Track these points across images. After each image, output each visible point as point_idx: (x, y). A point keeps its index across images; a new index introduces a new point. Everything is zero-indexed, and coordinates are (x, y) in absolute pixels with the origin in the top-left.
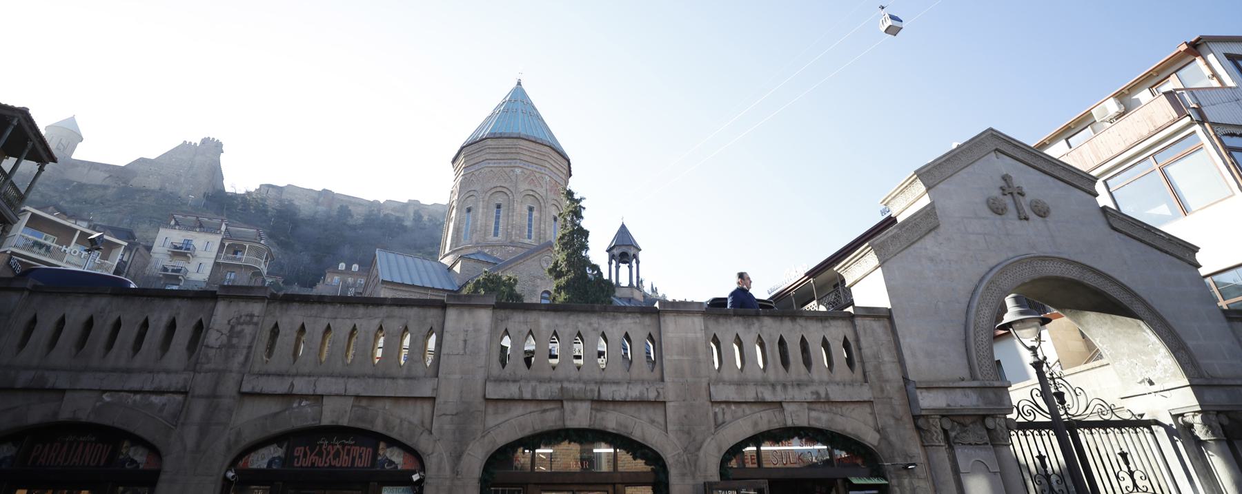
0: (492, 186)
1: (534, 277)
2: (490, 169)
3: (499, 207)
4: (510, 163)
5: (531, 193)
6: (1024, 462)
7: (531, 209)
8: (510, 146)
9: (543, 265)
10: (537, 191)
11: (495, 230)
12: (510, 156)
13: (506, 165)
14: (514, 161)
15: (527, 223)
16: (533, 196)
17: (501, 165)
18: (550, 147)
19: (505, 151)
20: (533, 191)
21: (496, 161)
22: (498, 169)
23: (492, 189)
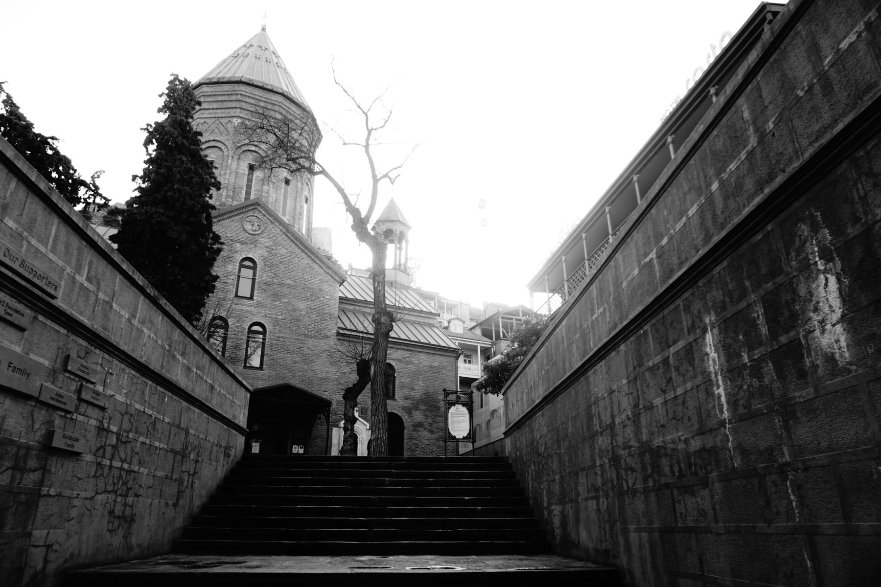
1: (232, 240)
2: (202, 121)
4: (229, 113)
5: (253, 148)
6: (402, 291)
8: (229, 93)
12: (229, 105)
14: (234, 110)
15: (245, 184)
17: (217, 116)
18: (282, 95)
19: (223, 98)
21: (211, 111)
22: (214, 120)
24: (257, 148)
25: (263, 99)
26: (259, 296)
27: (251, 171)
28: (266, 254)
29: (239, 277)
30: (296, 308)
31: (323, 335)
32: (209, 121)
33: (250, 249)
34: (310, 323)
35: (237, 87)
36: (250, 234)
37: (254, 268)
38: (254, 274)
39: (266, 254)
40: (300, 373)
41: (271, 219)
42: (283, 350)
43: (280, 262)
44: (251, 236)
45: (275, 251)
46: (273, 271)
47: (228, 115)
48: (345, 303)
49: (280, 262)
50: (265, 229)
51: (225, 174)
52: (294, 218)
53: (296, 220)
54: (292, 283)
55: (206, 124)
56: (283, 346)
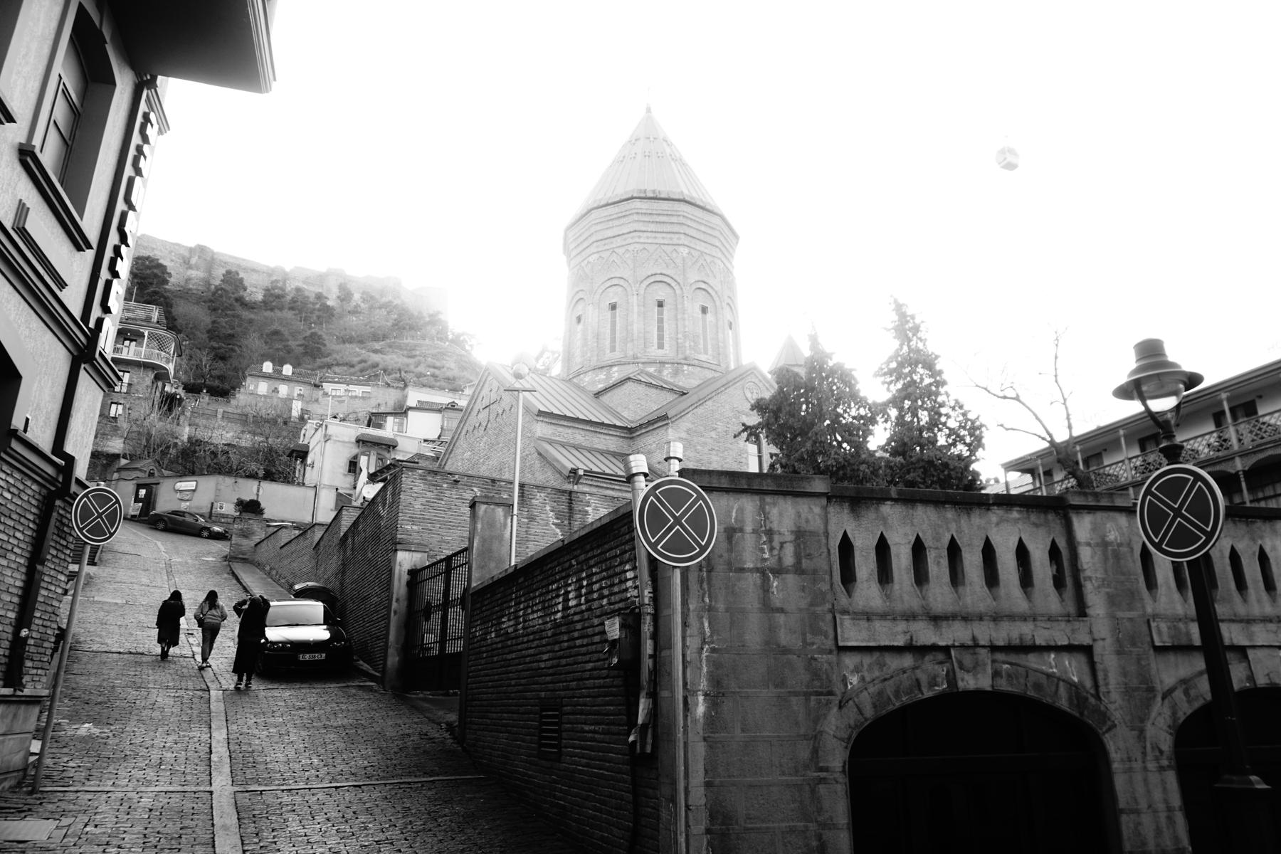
1: (739, 412)
2: (641, 247)
3: (660, 305)
4: (671, 239)
7: (704, 310)
8: (669, 213)
10: (710, 282)
11: (658, 339)
13: (650, 241)
14: (677, 236)
16: (704, 290)
17: (656, 241)
20: (705, 282)
21: (649, 234)
25: (704, 222)
35: (677, 206)
47: (671, 242)
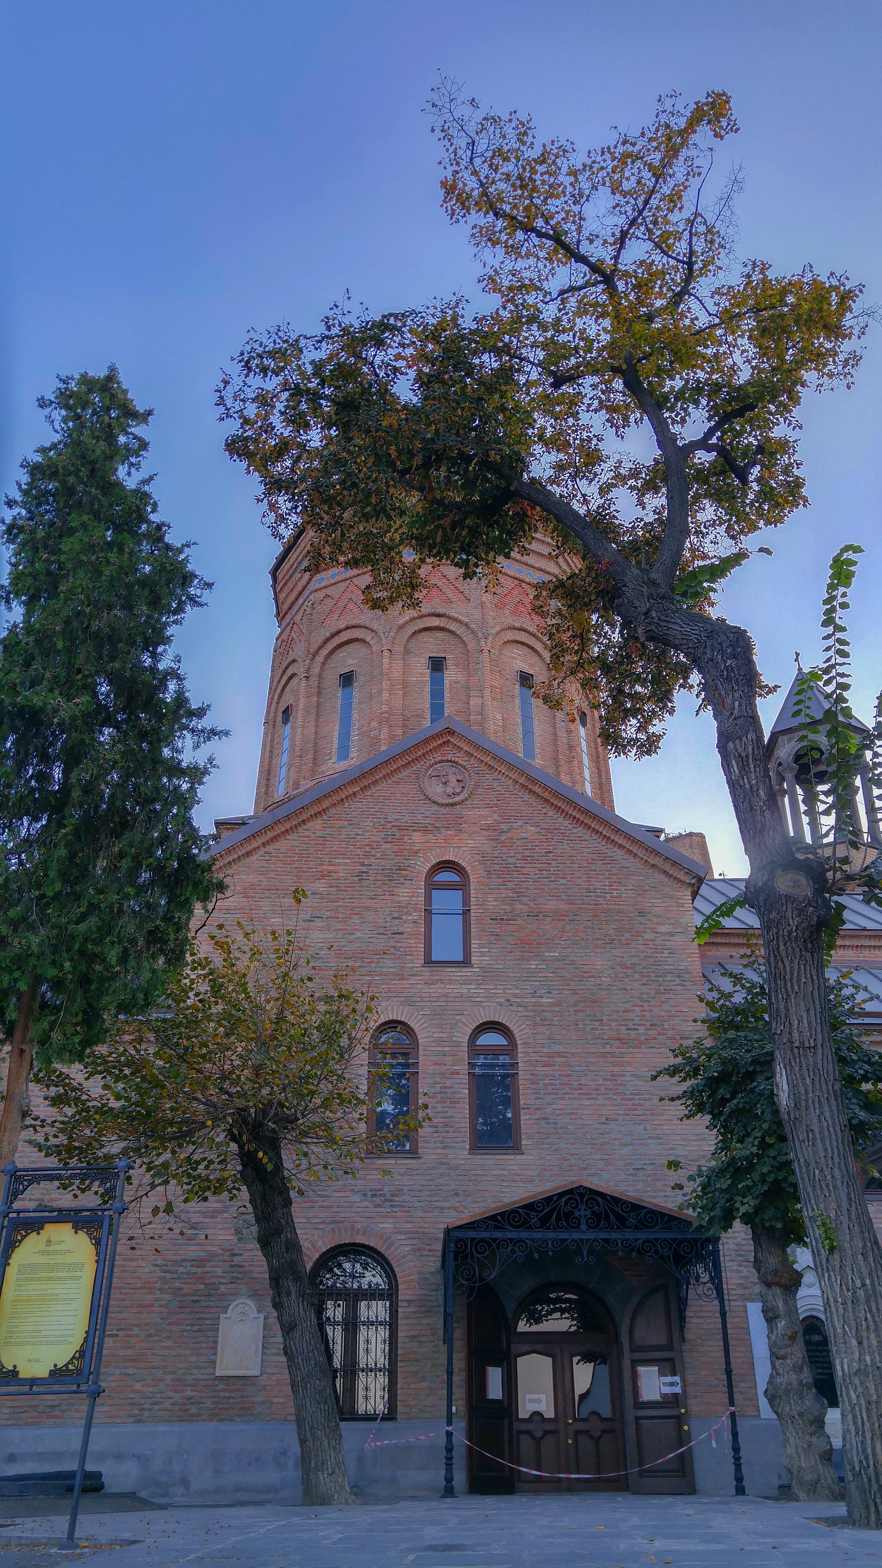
0: (328, 635)
1: (400, 828)
2: (320, 595)
5: (435, 622)
7: (437, 665)
9: (430, 791)
20: (439, 615)
22: (343, 585)
23: (327, 640)
24: (443, 619)
26: (483, 954)
27: (437, 674)
28: (487, 847)
29: (428, 912)
30: (585, 969)
31: (670, 1033)
32: (335, 591)
33: (446, 840)
34: (628, 1006)
36: (442, 805)
37: (463, 886)
38: (466, 901)
39: (487, 847)
40: (626, 1150)
41: (487, 760)
42: (567, 1089)
43: (525, 858)
44: (444, 810)
45: (509, 835)
46: (510, 885)
48: (722, 944)
49: (525, 858)
50: (477, 786)
51: (380, 692)
52: (556, 760)
53: (562, 763)
54: (564, 907)
55: (329, 600)
56: (565, 1079)
